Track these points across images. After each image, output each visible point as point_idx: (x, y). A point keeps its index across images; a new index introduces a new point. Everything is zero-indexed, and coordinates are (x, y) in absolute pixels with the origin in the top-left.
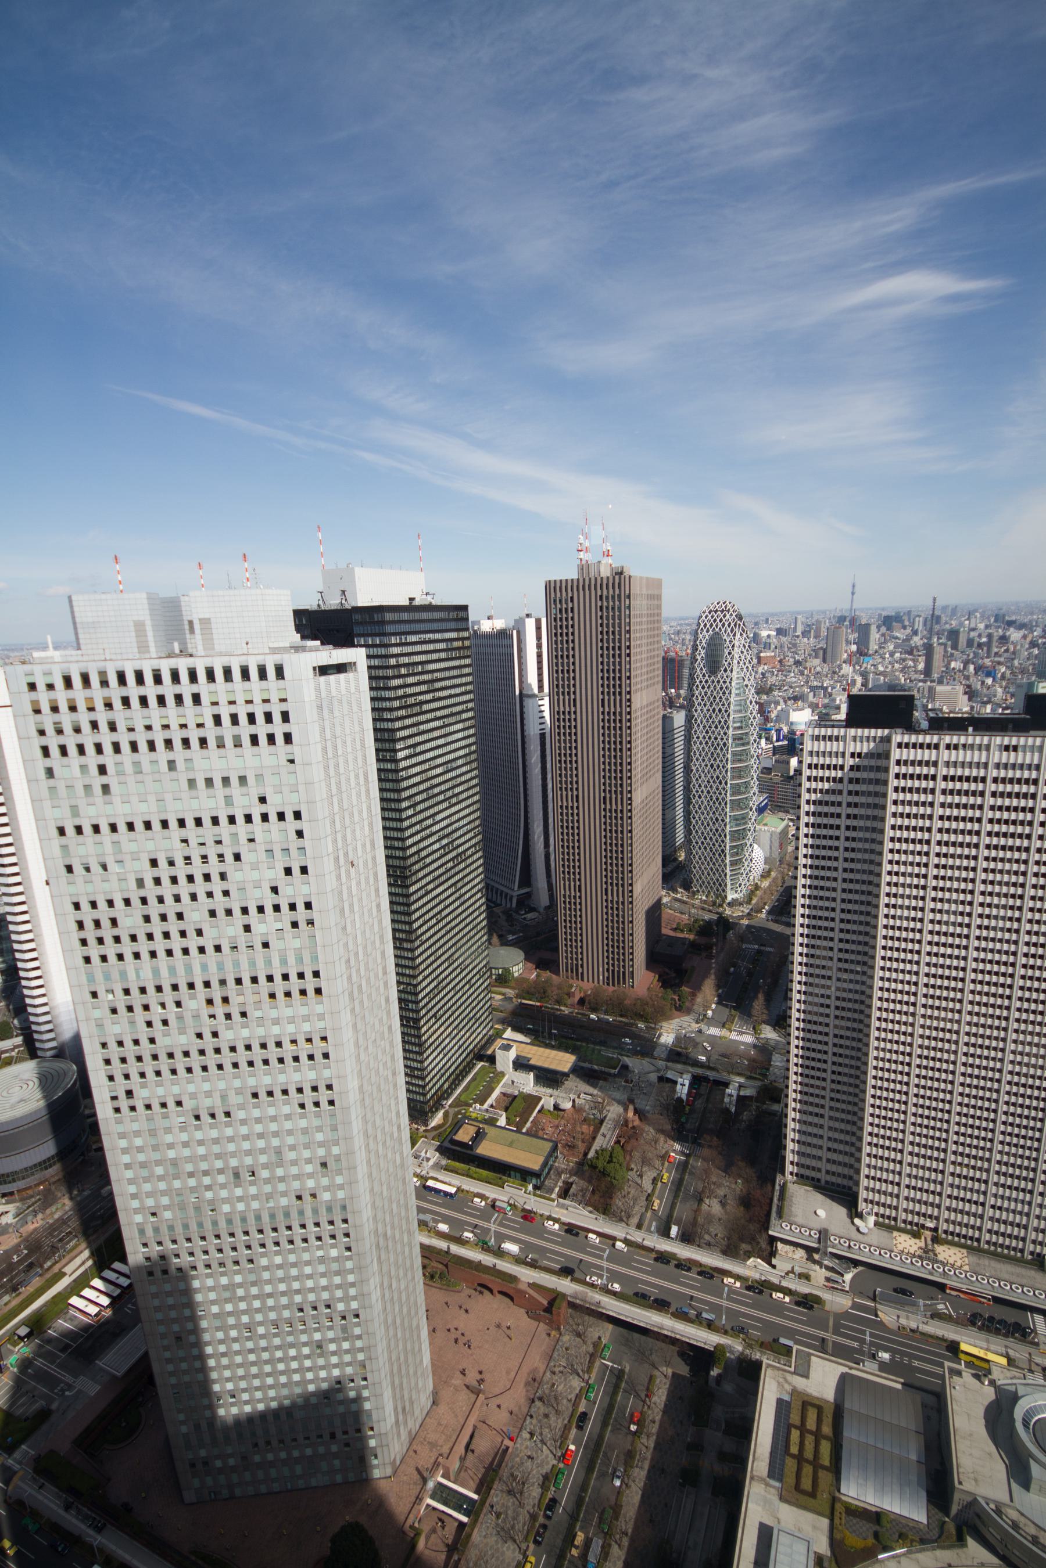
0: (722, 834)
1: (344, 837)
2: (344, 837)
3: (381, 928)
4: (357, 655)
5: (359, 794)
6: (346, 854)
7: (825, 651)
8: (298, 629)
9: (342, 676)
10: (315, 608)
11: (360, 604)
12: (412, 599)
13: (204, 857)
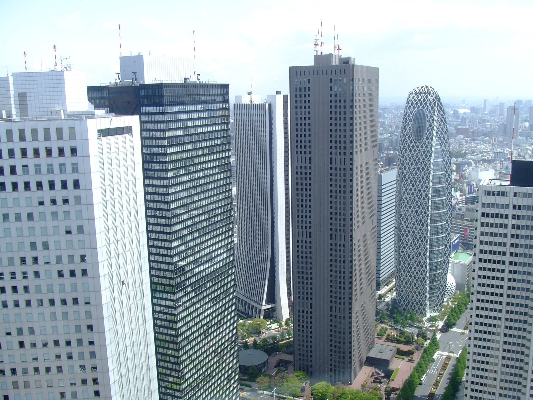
0: (424, 266)
1: (118, 262)
2: (118, 262)
3: (146, 334)
4: (133, 121)
5: (130, 228)
6: (119, 275)
7: (10, 121)
8: (90, 99)
9: (120, 137)
10: (113, 84)
11: (146, 82)
12: (185, 79)
13: (13, 274)
